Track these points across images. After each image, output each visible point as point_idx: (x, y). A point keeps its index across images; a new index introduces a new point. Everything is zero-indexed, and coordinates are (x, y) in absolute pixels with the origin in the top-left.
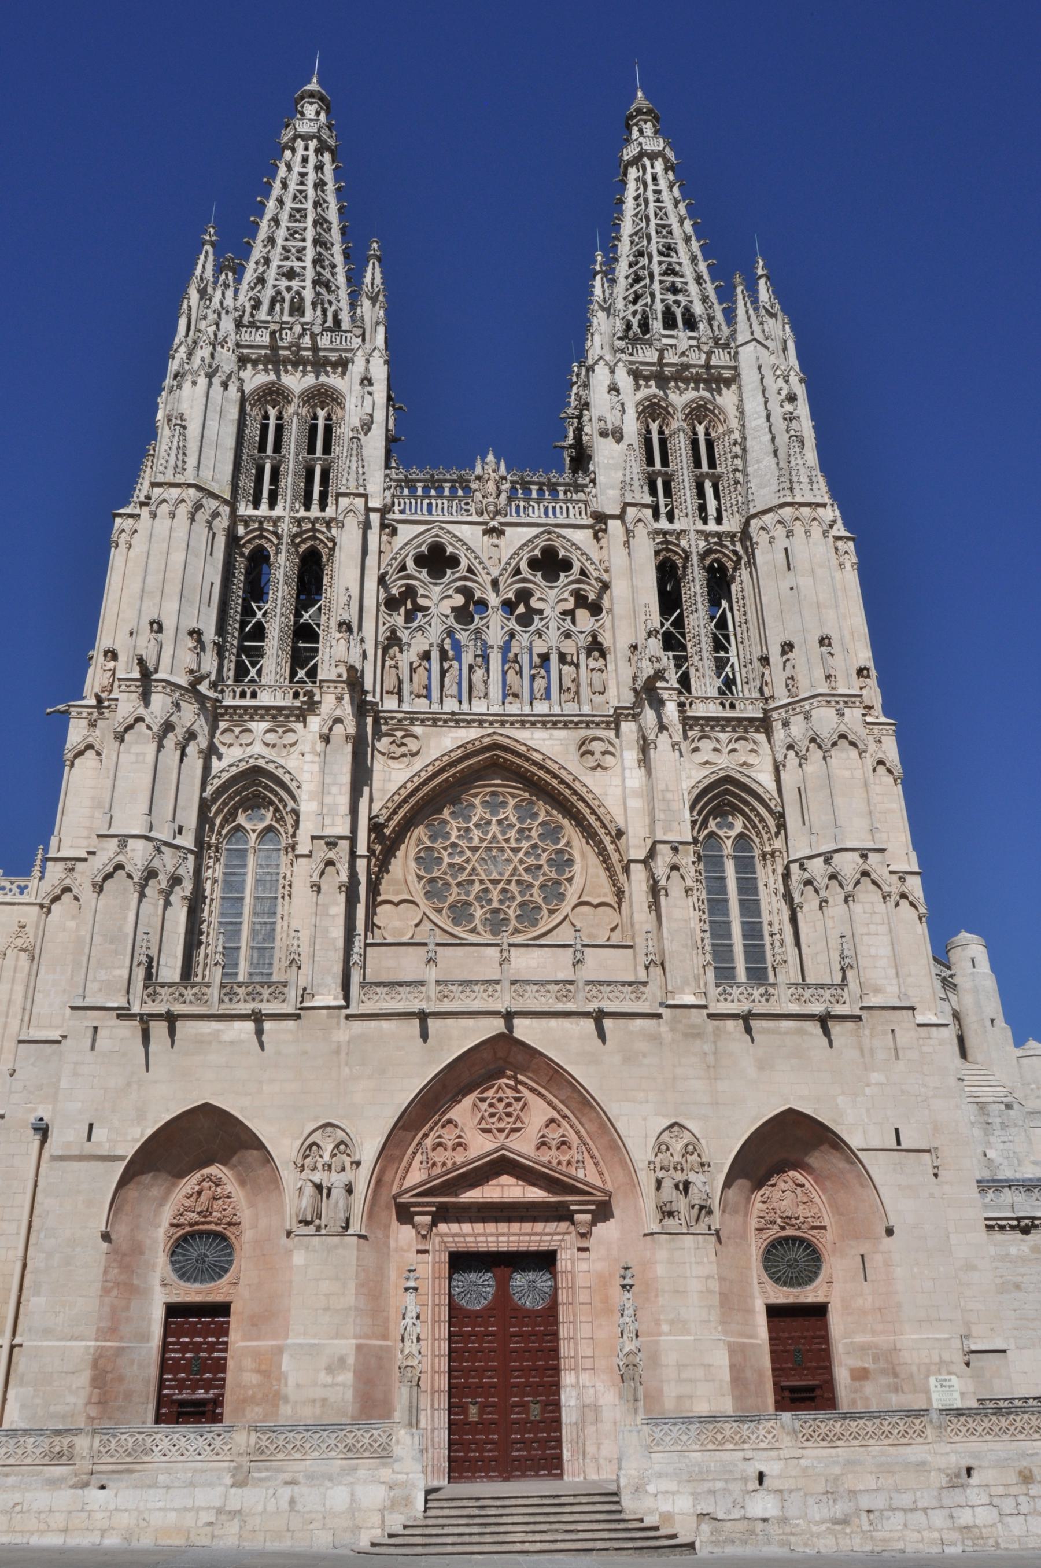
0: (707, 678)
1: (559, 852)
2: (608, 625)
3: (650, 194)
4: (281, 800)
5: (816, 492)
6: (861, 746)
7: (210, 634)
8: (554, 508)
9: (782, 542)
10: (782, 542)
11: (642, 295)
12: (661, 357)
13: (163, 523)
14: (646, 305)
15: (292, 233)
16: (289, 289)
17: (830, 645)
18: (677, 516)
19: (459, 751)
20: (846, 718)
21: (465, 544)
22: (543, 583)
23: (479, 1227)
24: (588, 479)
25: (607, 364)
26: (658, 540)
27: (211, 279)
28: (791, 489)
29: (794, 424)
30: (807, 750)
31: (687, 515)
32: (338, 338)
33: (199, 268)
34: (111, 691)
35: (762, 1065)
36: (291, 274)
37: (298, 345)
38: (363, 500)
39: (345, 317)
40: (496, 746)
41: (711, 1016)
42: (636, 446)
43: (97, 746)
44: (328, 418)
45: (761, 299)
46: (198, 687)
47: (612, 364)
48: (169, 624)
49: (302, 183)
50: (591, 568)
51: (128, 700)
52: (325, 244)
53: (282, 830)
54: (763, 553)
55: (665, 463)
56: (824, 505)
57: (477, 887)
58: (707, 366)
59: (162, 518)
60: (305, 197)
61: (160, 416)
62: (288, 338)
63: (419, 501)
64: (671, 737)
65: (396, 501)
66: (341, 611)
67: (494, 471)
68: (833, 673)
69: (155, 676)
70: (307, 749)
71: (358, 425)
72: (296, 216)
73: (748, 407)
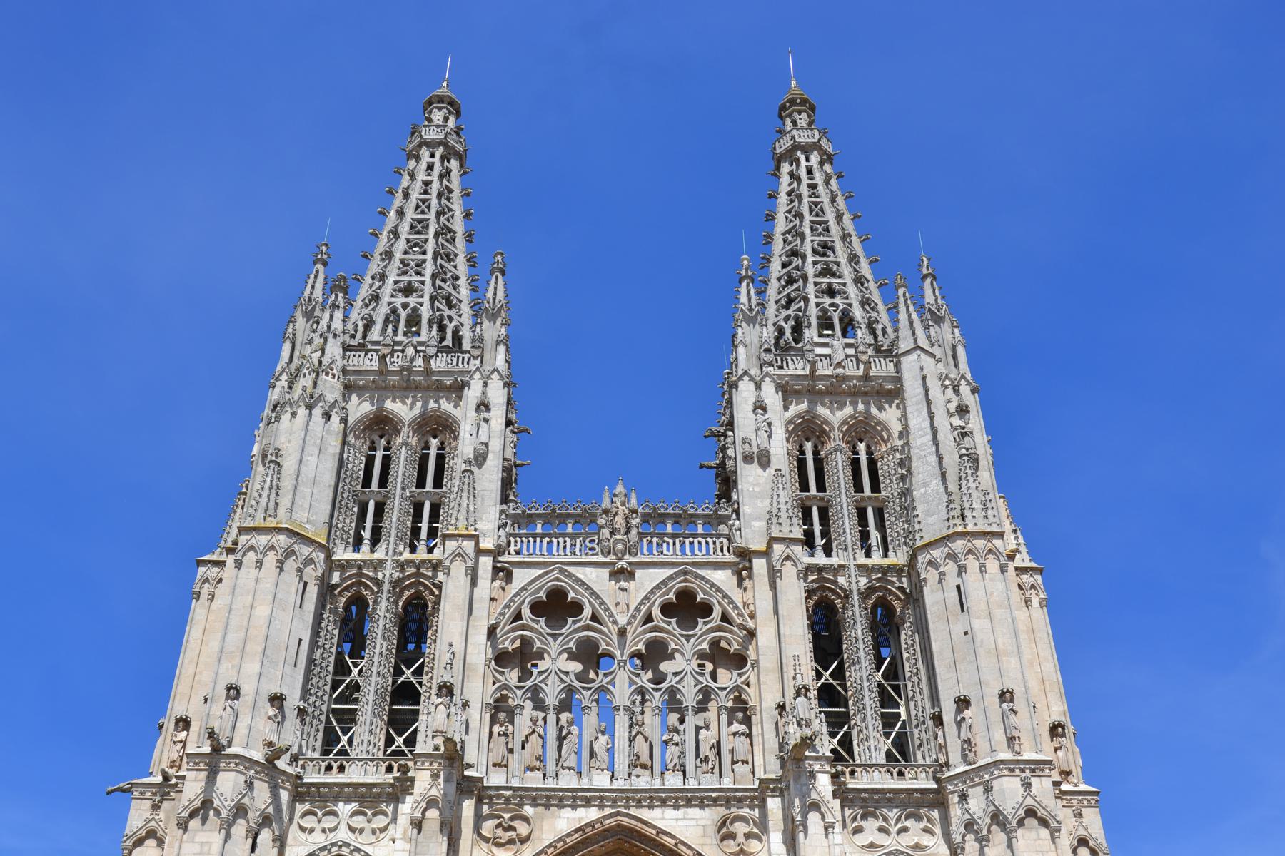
0: (872, 741)
2: (753, 680)
3: (804, 190)
5: (991, 519)
6: (1053, 824)
7: (293, 699)
8: (691, 543)
9: (952, 580)
10: (952, 580)
11: (795, 299)
12: (813, 370)
13: (248, 573)
14: (799, 309)
15: (412, 244)
16: (405, 306)
17: (1012, 701)
18: (835, 549)
19: (576, 836)
20: (1034, 790)
21: (589, 588)
22: (678, 632)
24: (730, 510)
25: (752, 379)
26: (811, 578)
27: (321, 300)
28: (963, 517)
29: (967, 442)
30: (989, 831)
31: (845, 550)
33: (309, 287)
34: (180, 767)
36: (408, 290)
37: (409, 369)
38: (473, 543)
39: (466, 333)
40: (620, 829)
42: (785, 471)
43: (160, 833)
45: (927, 300)
46: (276, 762)
47: (758, 379)
48: (247, 689)
49: (426, 192)
50: (733, 614)
51: (196, 780)
52: (448, 255)
55: (821, 487)
56: (1001, 535)
58: (866, 377)
59: (248, 567)
60: (429, 207)
61: (255, 450)
62: (396, 363)
63: (538, 539)
64: (823, 818)
65: (512, 540)
66: (442, 671)
67: (623, 504)
68: (1016, 734)
69: (228, 751)
70: (398, 835)
71: (472, 456)
72: (419, 226)
73: (912, 423)
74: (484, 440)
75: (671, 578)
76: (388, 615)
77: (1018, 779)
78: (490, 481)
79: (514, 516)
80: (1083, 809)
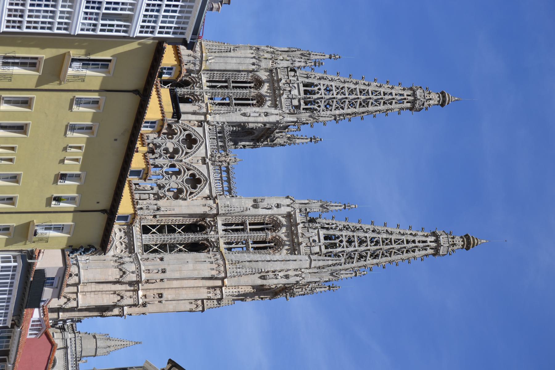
9: (208, 260)
20: (131, 274)
21: (197, 150)
32: (289, 104)
44: (253, 105)
50: (193, 195)
54: (205, 255)
63: (215, 135)
65: (214, 127)
74: (252, 115)
75: (204, 175)
76: (182, 92)
77: (135, 270)
78: (236, 118)
79: (223, 127)
80: (133, 299)
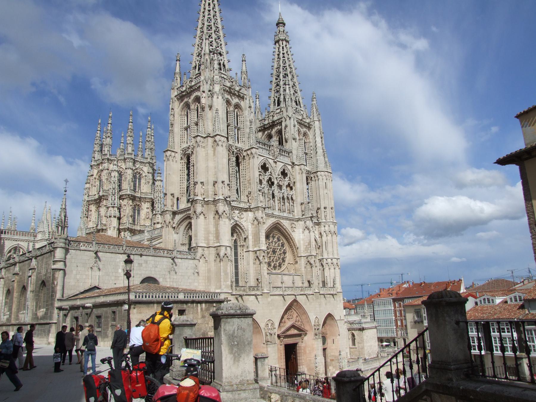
1: (284, 250)
2: (294, 194)
4: (240, 232)
10: (325, 181)
23: (288, 339)
35: (326, 304)
40: (278, 223)
41: (320, 294)
44: (237, 113)
50: (291, 177)
53: (239, 240)
57: (272, 258)
